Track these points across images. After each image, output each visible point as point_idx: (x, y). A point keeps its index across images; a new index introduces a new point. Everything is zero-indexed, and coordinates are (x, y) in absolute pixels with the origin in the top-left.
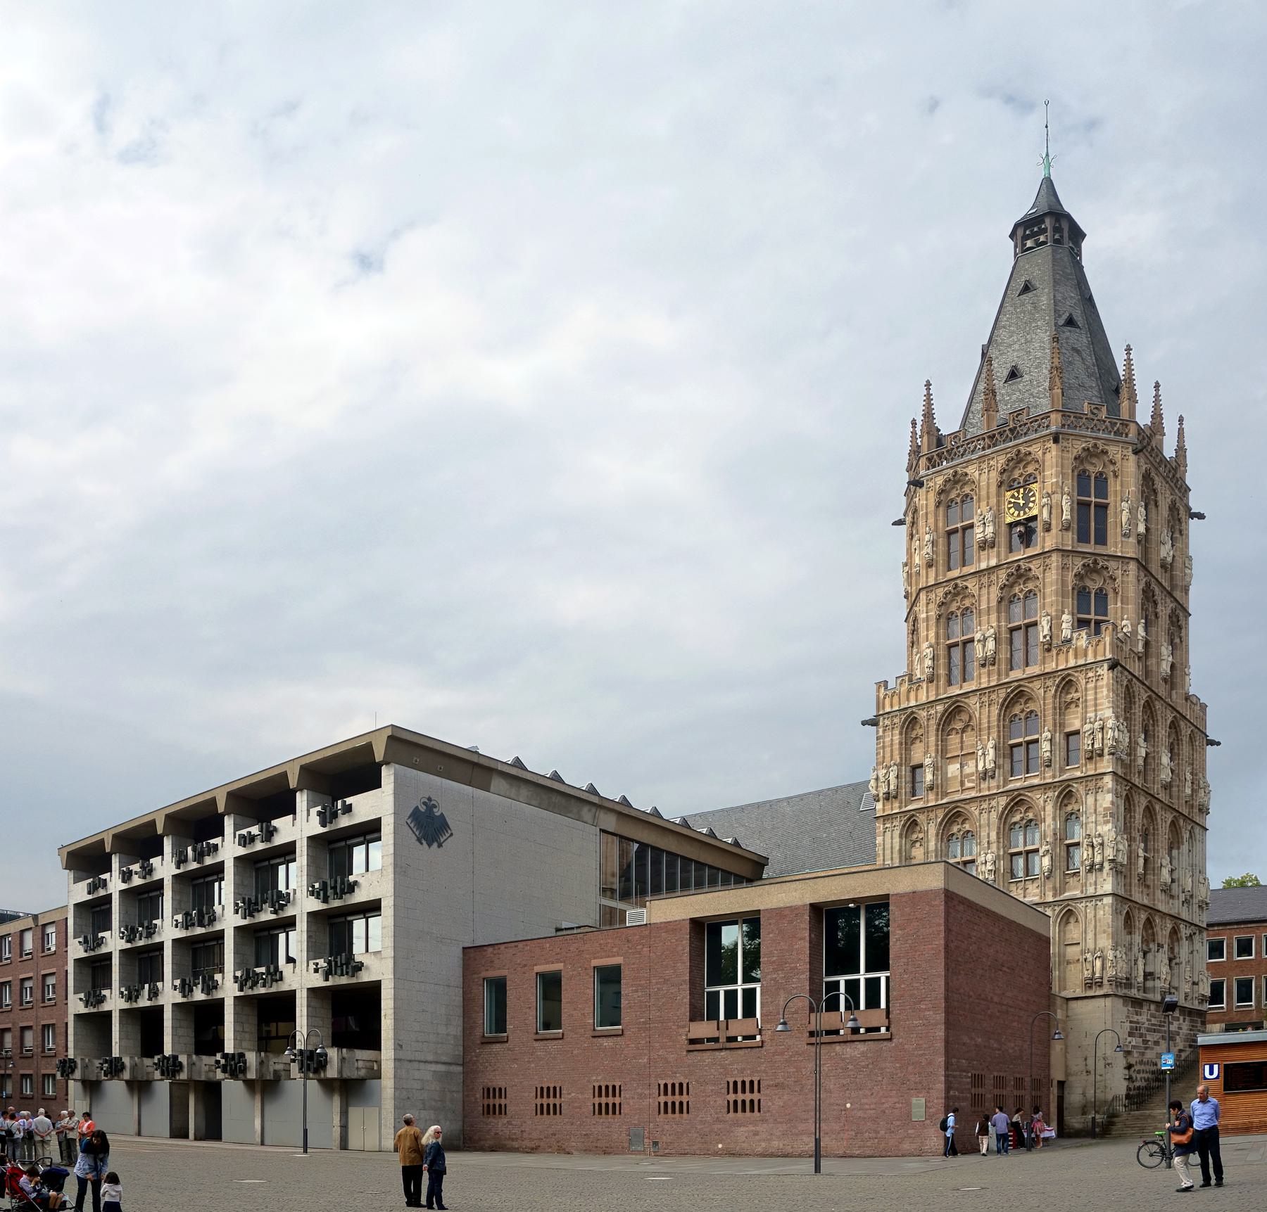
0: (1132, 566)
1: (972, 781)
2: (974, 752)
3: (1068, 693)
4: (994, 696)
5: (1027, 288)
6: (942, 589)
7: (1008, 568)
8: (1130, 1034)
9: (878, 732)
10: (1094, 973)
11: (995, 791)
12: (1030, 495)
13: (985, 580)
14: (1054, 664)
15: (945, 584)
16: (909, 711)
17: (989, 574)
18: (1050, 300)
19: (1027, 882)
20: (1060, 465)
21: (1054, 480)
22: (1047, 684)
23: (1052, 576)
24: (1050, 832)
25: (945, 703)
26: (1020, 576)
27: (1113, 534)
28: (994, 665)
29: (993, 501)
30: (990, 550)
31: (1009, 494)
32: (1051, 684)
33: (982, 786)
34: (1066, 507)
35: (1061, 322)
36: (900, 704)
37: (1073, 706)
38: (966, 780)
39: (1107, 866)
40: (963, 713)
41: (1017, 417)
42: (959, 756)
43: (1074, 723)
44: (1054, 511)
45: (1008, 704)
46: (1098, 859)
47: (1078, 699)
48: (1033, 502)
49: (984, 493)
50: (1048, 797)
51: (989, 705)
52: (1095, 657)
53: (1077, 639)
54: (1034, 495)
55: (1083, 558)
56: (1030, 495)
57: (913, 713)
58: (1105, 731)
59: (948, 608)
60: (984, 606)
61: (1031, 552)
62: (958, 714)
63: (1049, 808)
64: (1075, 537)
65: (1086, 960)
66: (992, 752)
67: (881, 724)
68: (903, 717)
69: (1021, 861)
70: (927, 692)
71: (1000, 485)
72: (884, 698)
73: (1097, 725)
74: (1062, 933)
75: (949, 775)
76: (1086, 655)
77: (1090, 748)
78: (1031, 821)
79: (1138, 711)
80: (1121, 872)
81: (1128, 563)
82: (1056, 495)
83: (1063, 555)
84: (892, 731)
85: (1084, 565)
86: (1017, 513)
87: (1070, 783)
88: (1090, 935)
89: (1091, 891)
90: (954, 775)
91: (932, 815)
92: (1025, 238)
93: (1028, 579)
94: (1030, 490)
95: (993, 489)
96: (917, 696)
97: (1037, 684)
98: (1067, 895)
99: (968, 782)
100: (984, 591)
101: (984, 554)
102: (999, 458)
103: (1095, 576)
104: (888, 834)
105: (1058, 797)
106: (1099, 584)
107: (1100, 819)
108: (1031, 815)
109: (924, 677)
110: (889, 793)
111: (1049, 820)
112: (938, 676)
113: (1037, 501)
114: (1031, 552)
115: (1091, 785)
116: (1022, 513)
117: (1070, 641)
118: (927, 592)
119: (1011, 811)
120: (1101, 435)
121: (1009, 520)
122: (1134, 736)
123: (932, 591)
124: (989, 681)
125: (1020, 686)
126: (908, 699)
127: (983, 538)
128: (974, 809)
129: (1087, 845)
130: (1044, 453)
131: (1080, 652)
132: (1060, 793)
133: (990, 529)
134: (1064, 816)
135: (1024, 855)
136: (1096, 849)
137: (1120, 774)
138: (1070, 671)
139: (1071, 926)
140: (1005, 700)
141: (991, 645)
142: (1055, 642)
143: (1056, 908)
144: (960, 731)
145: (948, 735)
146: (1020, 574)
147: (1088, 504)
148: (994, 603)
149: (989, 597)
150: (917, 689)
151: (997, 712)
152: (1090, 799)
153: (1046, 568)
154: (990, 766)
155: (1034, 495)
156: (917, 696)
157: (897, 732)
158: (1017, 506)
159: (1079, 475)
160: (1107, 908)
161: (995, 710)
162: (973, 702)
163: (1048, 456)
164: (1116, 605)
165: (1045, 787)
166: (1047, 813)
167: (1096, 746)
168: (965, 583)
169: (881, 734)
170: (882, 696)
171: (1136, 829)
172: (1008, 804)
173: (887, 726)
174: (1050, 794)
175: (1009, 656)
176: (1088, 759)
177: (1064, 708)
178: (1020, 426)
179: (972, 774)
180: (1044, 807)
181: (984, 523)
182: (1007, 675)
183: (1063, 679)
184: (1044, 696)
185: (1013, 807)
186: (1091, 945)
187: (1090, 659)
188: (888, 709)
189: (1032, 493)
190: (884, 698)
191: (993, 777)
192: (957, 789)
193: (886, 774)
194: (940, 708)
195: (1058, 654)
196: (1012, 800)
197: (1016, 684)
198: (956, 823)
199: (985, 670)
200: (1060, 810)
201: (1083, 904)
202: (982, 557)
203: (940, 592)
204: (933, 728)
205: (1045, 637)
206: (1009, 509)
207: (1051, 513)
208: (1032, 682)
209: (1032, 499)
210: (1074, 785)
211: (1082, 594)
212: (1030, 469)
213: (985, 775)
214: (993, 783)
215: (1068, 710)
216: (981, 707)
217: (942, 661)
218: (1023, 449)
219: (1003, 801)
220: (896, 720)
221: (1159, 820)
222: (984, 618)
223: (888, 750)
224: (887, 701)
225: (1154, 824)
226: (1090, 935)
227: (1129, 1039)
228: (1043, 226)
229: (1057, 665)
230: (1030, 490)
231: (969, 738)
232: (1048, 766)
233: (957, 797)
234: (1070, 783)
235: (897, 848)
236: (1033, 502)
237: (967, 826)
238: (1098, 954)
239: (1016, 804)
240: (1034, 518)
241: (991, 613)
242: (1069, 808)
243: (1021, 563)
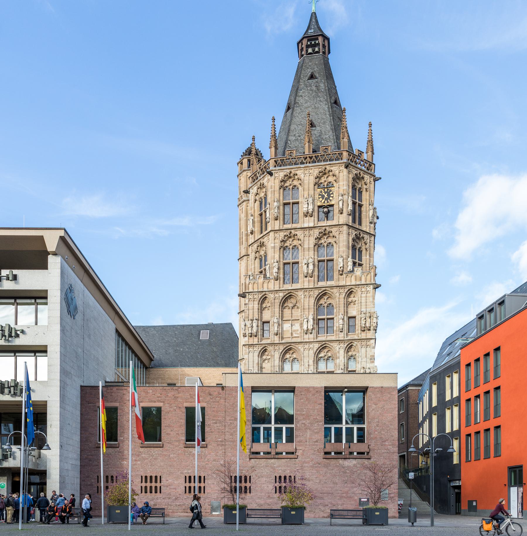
1: (298, 334)
6: (283, 233)
9: (245, 301)
11: (312, 340)
12: (330, 193)
13: (307, 232)
14: (345, 281)
15: (284, 231)
16: (264, 293)
17: (309, 230)
18: (326, 87)
20: (347, 180)
21: (345, 188)
22: (340, 292)
25: (284, 292)
28: (312, 277)
29: (312, 192)
30: (310, 218)
31: (319, 190)
32: (343, 291)
33: (305, 337)
37: (352, 304)
38: (294, 333)
40: (292, 299)
42: (290, 320)
43: (353, 312)
44: (345, 204)
47: (355, 301)
48: (332, 197)
49: (306, 187)
50: (341, 347)
51: (309, 297)
52: (366, 281)
53: (357, 271)
54: (332, 194)
56: (330, 193)
58: (371, 318)
60: (306, 246)
62: (290, 299)
63: (342, 352)
66: (312, 320)
67: (247, 297)
68: (260, 296)
72: (249, 284)
73: (368, 315)
76: (361, 280)
77: (364, 325)
82: (346, 196)
84: (253, 302)
87: (353, 341)
90: (287, 329)
91: (277, 348)
92: (308, 47)
94: (331, 191)
95: (312, 186)
97: (335, 290)
99: (295, 334)
104: (251, 354)
107: (368, 360)
108: (329, 354)
110: (252, 334)
113: (334, 197)
115: (364, 343)
117: (353, 271)
119: (319, 351)
123: (277, 233)
125: (326, 290)
127: (307, 211)
138: (353, 287)
142: (345, 271)
144: (291, 308)
145: (284, 309)
148: (312, 246)
149: (309, 242)
151: (313, 301)
154: (310, 327)
155: (332, 194)
157: (256, 303)
158: (323, 197)
162: (300, 294)
169: (247, 302)
170: (247, 283)
173: (250, 299)
174: (342, 345)
176: (362, 331)
177: (348, 304)
181: (308, 203)
182: (318, 284)
185: (321, 349)
187: (363, 282)
188: (251, 290)
189: (332, 192)
191: (311, 333)
192: (289, 336)
195: (346, 277)
197: (324, 289)
198: (288, 353)
199: (307, 279)
200: (347, 354)
202: (305, 221)
206: (319, 198)
207: (343, 205)
208: (333, 289)
209: (332, 195)
210: (355, 342)
214: (311, 336)
215: (349, 306)
217: (282, 271)
219: (317, 346)
220: (255, 297)
228: (317, 42)
230: (331, 191)
232: (341, 332)
233: (290, 340)
234: (353, 341)
235: (256, 362)
236: (332, 197)
237: (294, 356)
241: (310, 250)
242: (350, 353)
243: (327, 228)
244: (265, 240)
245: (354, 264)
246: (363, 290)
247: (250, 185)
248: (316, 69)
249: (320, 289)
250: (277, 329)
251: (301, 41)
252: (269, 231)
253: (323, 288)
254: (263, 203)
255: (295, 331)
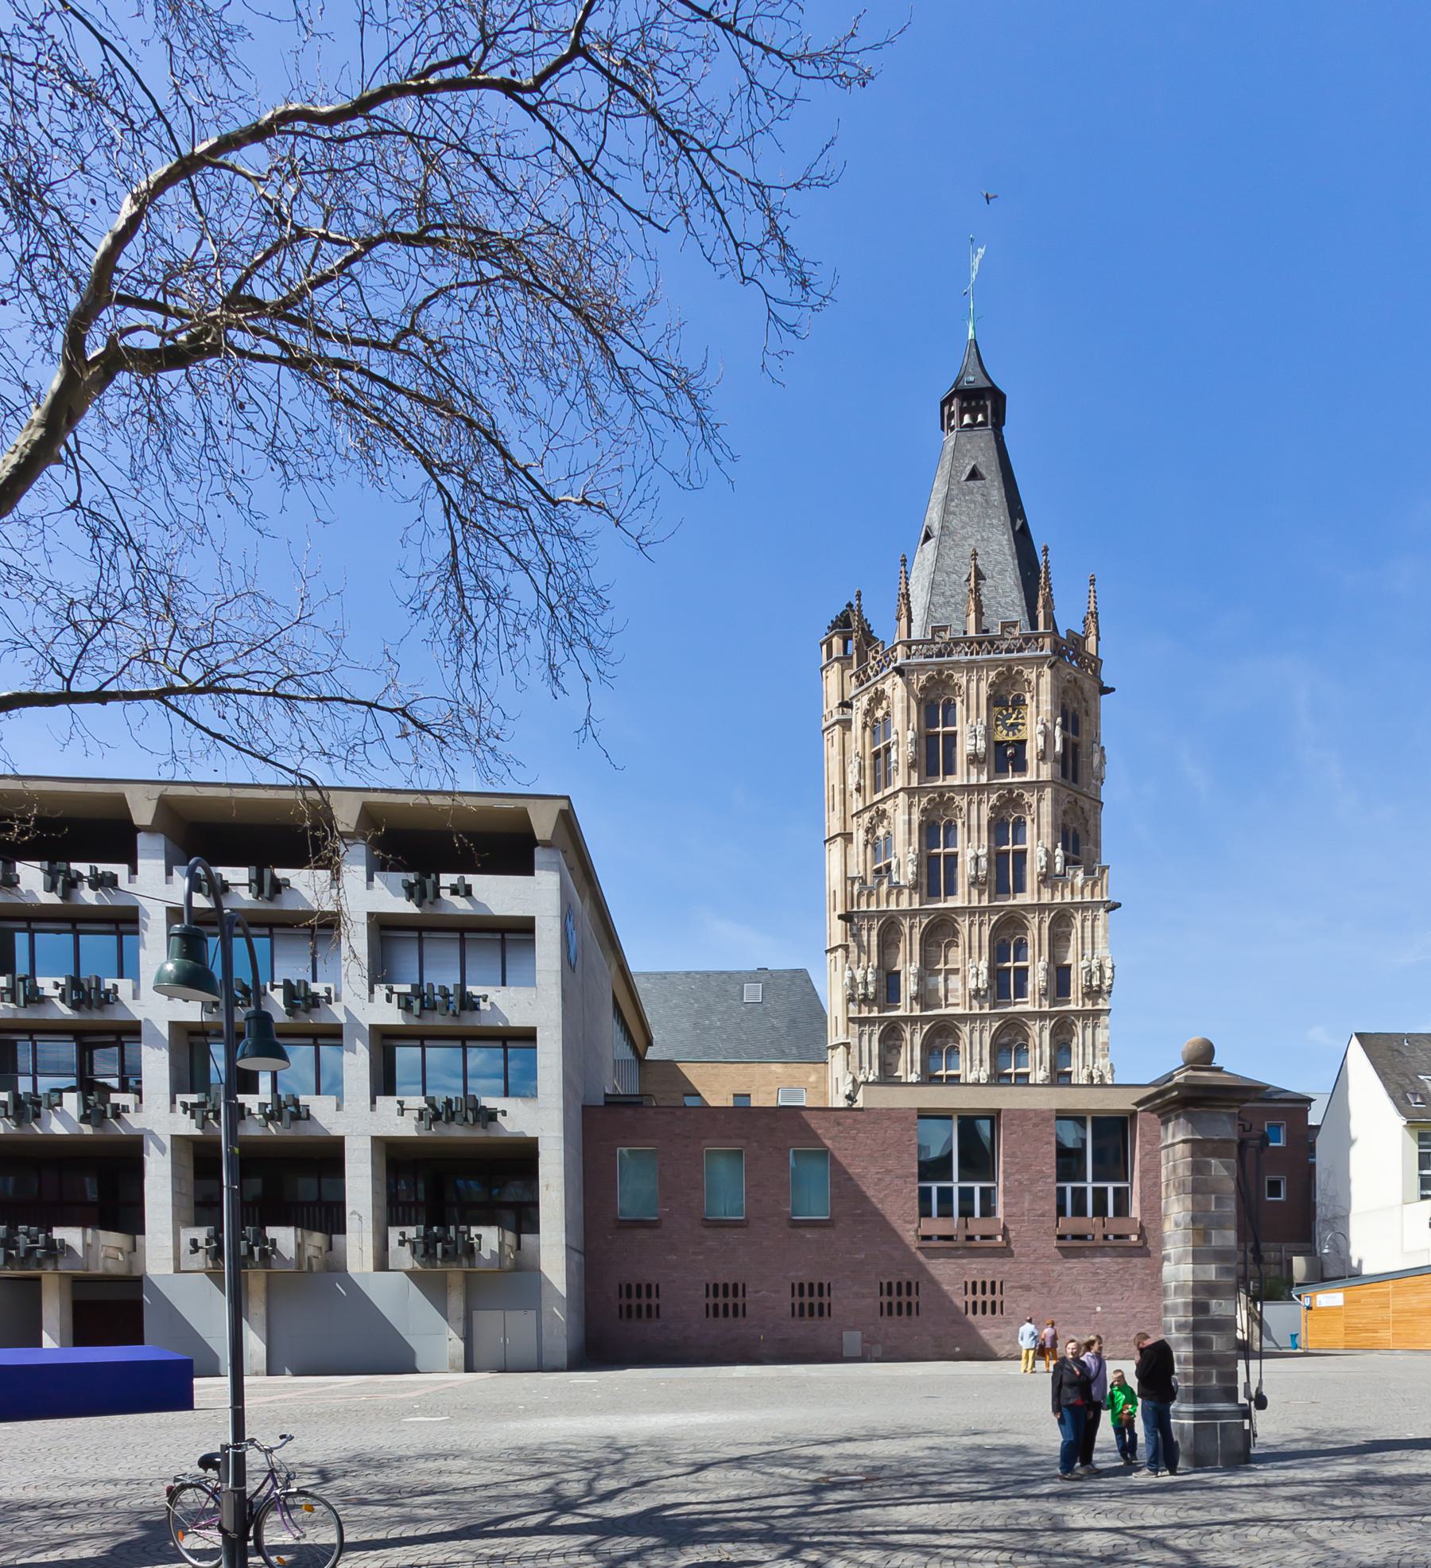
1: (957, 997)
3: (1060, 926)
5: (974, 475)
23: (1046, 807)
112: (921, 884)
217: (925, 870)
224: (864, 899)
244: (888, 806)
245: (1067, 862)
247: (853, 692)
248: (981, 459)
251: (947, 401)
252: (897, 788)
254: (877, 727)
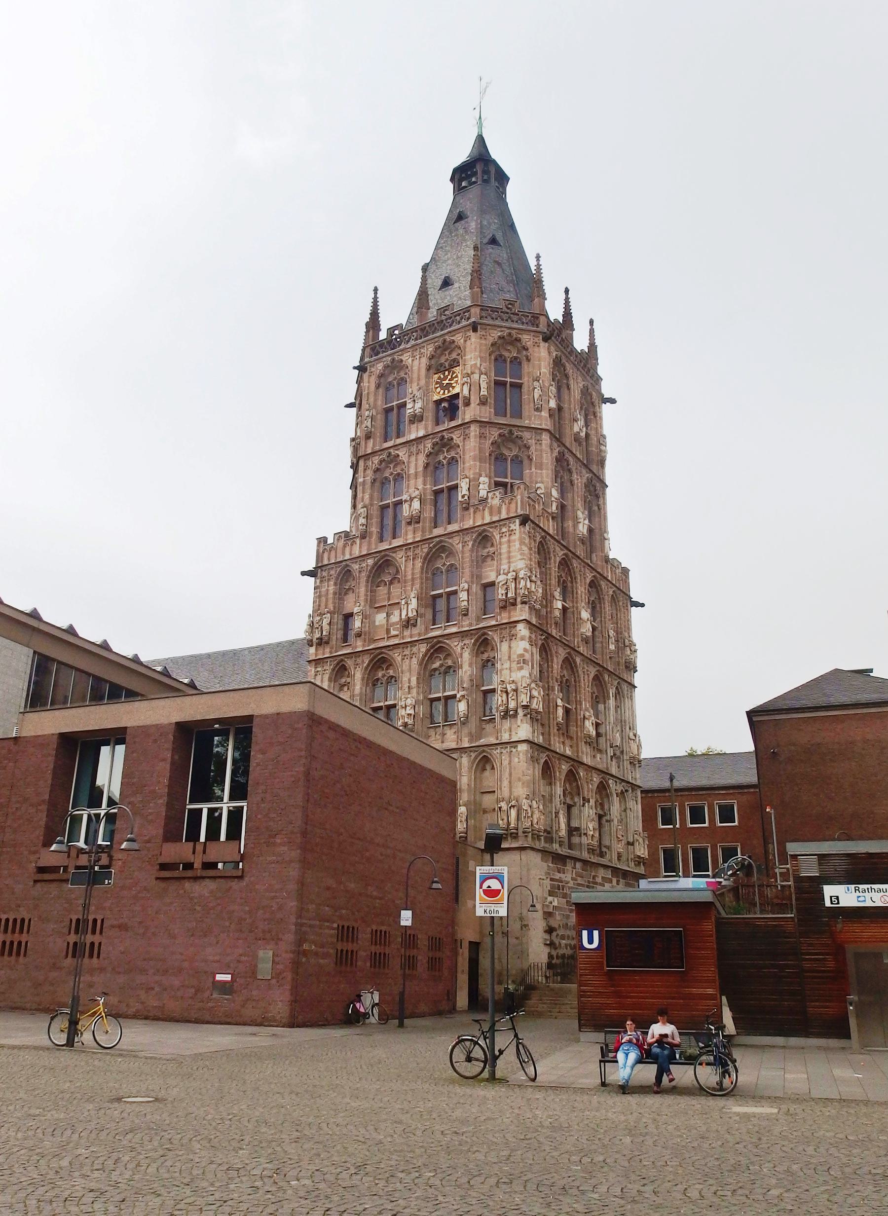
0: (545, 437)
2: (399, 603)
4: (418, 551)
6: (377, 457)
7: (433, 438)
8: (551, 894)
9: (315, 582)
10: (509, 823)
13: (414, 449)
15: (379, 453)
17: (417, 443)
19: (445, 728)
22: (465, 540)
24: (466, 679)
25: (375, 557)
26: (444, 445)
27: (527, 409)
28: (419, 522)
29: (423, 382)
31: (436, 376)
33: (405, 633)
34: (484, 385)
35: (485, 241)
36: (336, 557)
37: (489, 559)
39: (520, 712)
41: (444, 312)
43: (491, 576)
45: (429, 559)
46: (512, 705)
47: (494, 553)
49: (415, 376)
50: (465, 644)
53: (492, 498)
55: (500, 428)
57: (347, 565)
59: (383, 474)
61: (453, 424)
63: (466, 655)
64: (492, 410)
65: (500, 808)
67: (319, 575)
68: (339, 569)
69: (440, 706)
70: (360, 547)
71: (429, 368)
72: (323, 552)
73: (511, 576)
74: (478, 781)
75: (377, 623)
78: (450, 667)
79: (554, 566)
80: (537, 720)
81: (541, 434)
83: (480, 426)
85: (500, 435)
86: (442, 391)
88: (506, 783)
89: (505, 737)
91: (359, 660)
93: (451, 448)
95: (423, 371)
96: (351, 550)
98: (483, 741)
100: (413, 459)
101: (414, 427)
102: (429, 346)
103: (511, 445)
105: (474, 644)
106: (514, 453)
108: (450, 662)
109: (358, 534)
111: (466, 667)
112: (371, 533)
114: (453, 424)
115: (506, 633)
116: (446, 391)
118: (365, 460)
119: (430, 657)
120: (515, 325)
121: (436, 398)
122: (550, 589)
124: (414, 538)
125: (441, 541)
126: (343, 554)
128: (397, 656)
129: (501, 691)
130: (465, 341)
131: (495, 510)
132: (476, 641)
133: (419, 405)
134: (481, 663)
135: (443, 700)
136: (510, 695)
137: (534, 623)
139: (487, 773)
140: (428, 554)
141: (416, 504)
143: (472, 754)
146: (444, 444)
147: (504, 384)
148: (421, 469)
149: (415, 463)
150: (352, 545)
151: (420, 564)
152: (504, 647)
153: (466, 437)
156: (351, 550)
159: (496, 359)
160: (521, 754)
161: (419, 564)
162: (400, 556)
163: (468, 343)
164: (531, 469)
165: (462, 635)
166: (464, 660)
167: (509, 595)
168: (397, 452)
169: (318, 584)
171: (554, 679)
172: (428, 651)
175: (433, 515)
177: (481, 561)
178: (446, 319)
179: (397, 623)
180: (462, 654)
181: (414, 401)
182: (431, 532)
183: (480, 534)
184: (463, 549)
185: (432, 654)
186: (506, 793)
187: (504, 515)
188: (326, 562)
190: (323, 552)
193: (320, 620)
194: (370, 562)
196: (432, 647)
199: (410, 528)
201: (498, 751)
203: (376, 459)
204: (363, 580)
205: (463, 497)
211: (498, 459)
212: (454, 356)
213: (408, 623)
215: (485, 563)
216: (406, 561)
218: (448, 338)
219: (423, 648)
220: (332, 572)
221: (580, 672)
222: (412, 482)
223: (324, 599)
225: (575, 677)
226: (506, 783)
227: (550, 899)
229: (474, 522)
231: (396, 590)
233: (381, 644)
238: (513, 803)
239: (436, 651)
240: (457, 396)
242: (485, 656)
246: (504, 530)
249: (430, 541)
250: (360, 626)
253: (435, 540)
255: (394, 624)
